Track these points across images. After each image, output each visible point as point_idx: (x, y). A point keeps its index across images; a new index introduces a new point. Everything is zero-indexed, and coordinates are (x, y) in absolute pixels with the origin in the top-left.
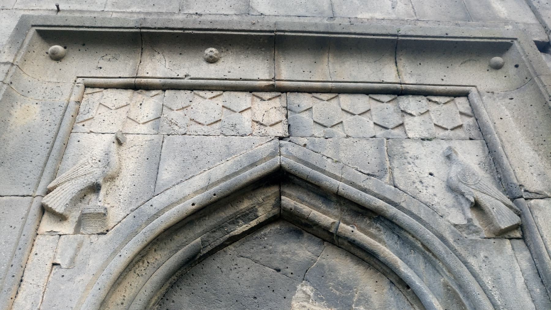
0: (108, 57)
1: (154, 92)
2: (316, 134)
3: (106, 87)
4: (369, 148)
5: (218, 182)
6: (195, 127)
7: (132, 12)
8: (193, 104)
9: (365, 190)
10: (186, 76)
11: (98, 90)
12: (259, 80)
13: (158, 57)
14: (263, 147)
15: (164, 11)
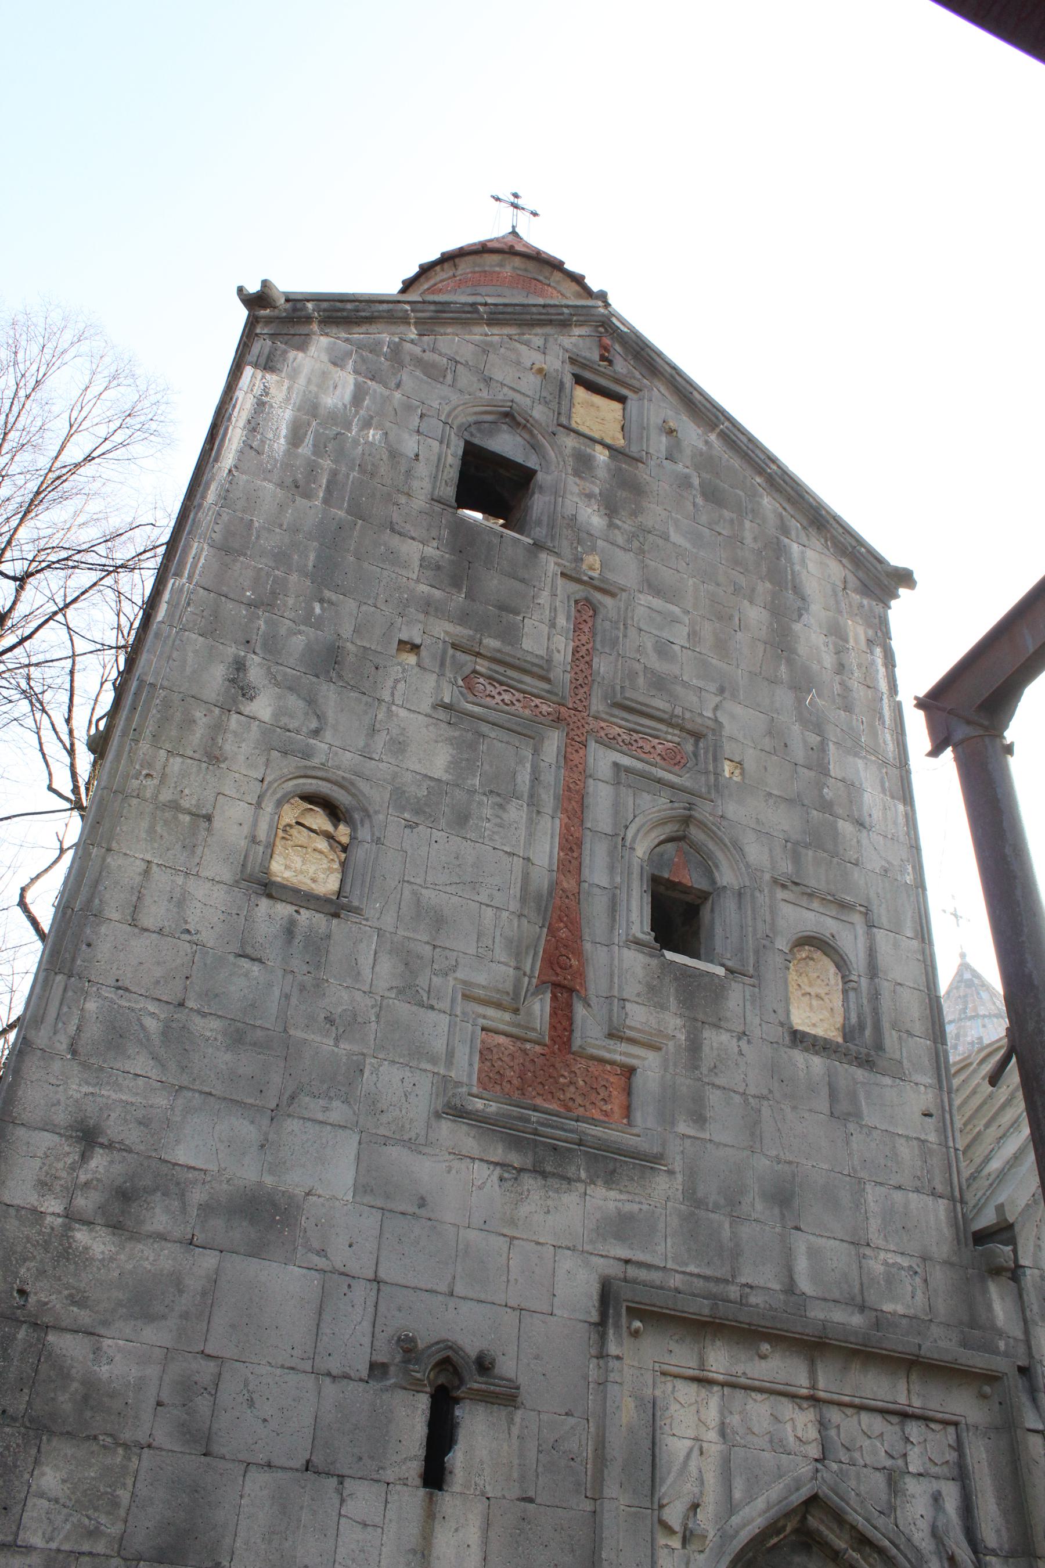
0: (676, 1337)
1: (716, 1388)
2: (843, 1459)
3: (675, 1377)
4: (880, 1478)
5: (775, 1506)
6: (750, 1437)
7: (691, 1274)
8: (748, 1407)
9: (875, 1528)
10: (744, 1373)
11: (669, 1378)
12: (801, 1387)
13: (718, 1343)
14: (805, 1469)
15: (719, 1276)
